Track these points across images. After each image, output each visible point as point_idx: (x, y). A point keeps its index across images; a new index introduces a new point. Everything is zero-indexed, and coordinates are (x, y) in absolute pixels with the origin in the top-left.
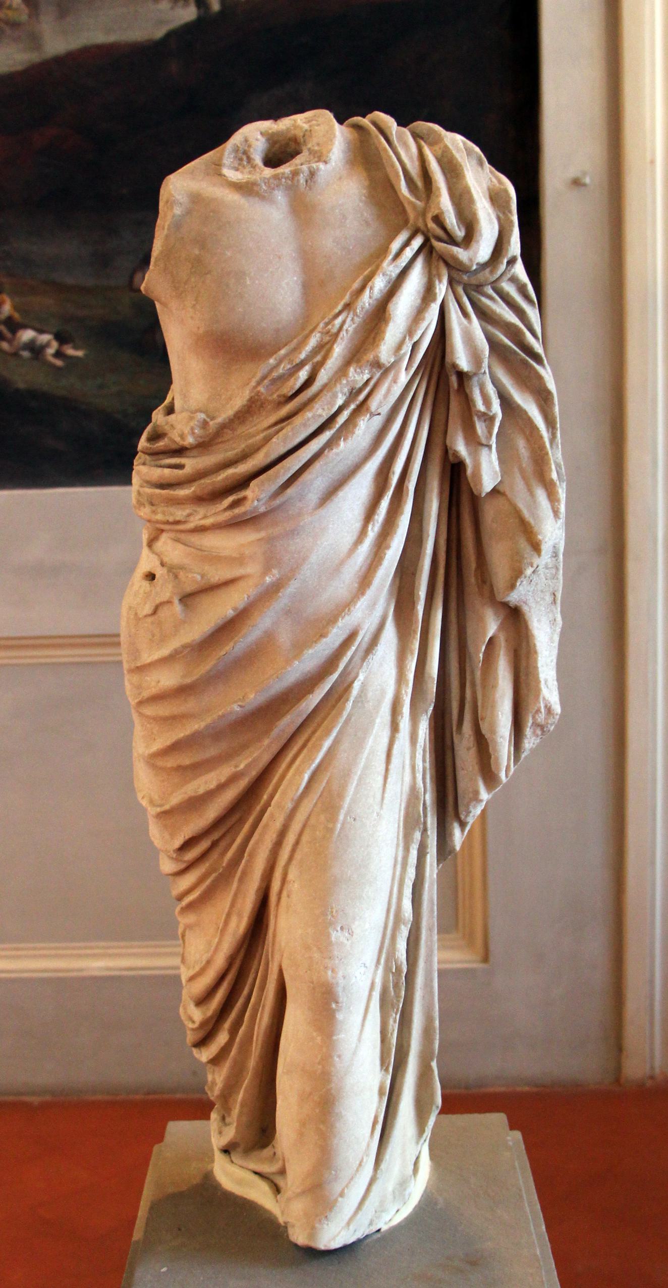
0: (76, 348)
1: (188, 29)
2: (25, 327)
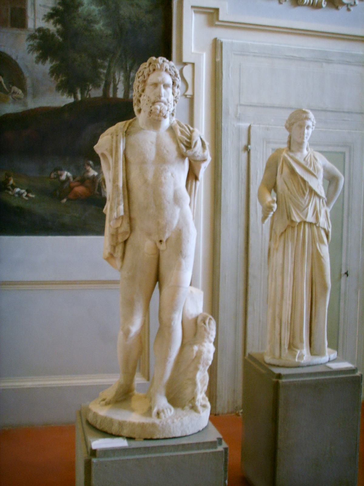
0: (32, 194)
1: (71, 104)
2: (17, 187)
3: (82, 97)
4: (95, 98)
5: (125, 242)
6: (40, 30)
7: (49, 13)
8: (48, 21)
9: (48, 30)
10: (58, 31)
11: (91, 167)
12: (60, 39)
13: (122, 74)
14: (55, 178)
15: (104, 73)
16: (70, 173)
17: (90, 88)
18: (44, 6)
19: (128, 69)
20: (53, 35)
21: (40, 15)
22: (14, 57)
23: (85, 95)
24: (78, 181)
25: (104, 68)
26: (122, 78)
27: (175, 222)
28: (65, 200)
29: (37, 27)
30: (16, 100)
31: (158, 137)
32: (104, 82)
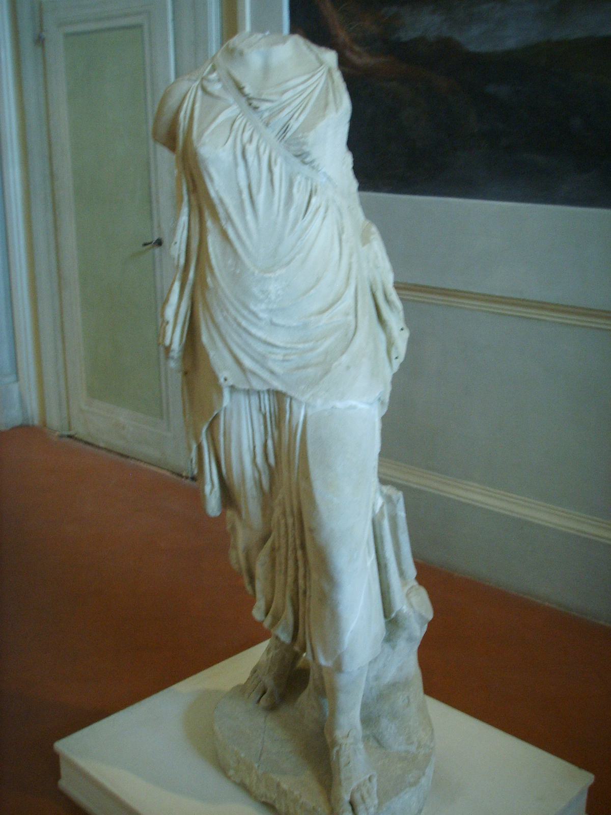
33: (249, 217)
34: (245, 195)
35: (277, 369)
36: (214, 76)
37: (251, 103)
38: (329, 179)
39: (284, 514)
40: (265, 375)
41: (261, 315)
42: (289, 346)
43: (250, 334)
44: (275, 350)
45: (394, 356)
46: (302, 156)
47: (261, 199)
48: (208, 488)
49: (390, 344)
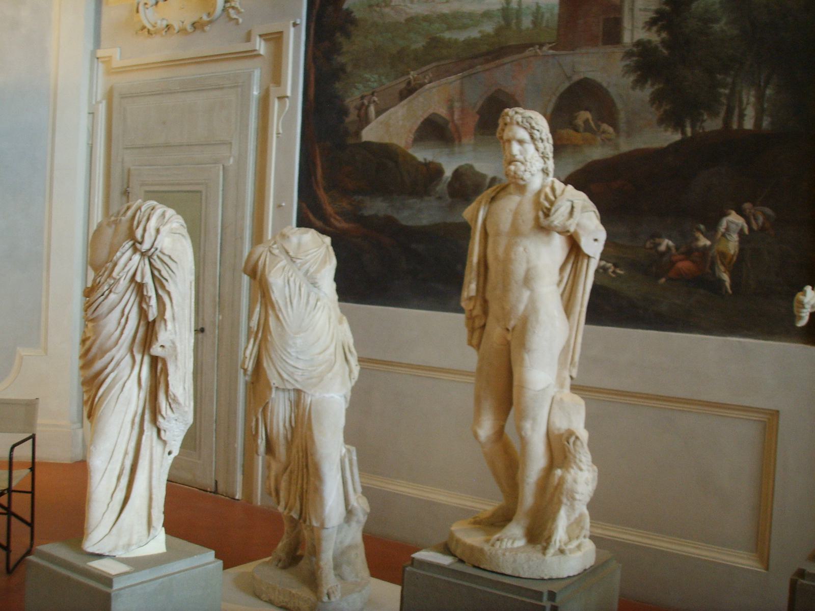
1: (676, 144)
3: (692, 132)
4: (712, 132)
5: (483, 327)
6: (639, 43)
7: (651, 18)
8: (649, 29)
9: (649, 42)
10: (663, 42)
11: (702, 233)
12: (665, 52)
13: (753, 93)
14: (651, 249)
15: (725, 94)
16: (672, 241)
17: (705, 117)
18: (645, 10)
19: (762, 84)
20: (656, 47)
21: (640, 23)
22: (605, 85)
23: (698, 129)
24: (683, 253)
25: (725, 86)
26: (752, 99)
27: (522, 307)
28: (663, 280)
29: (635, 40)
30: (606, 141)
31: (520, 204)
32: (725, 108)
33: (289, 310)
34: (288, 300)
35: (299, 379)
36: (275, 246)
37: (292, 260)
38: (326, 294)
39: (298, 452)
40: (293, 382)
41: (293, 354)
42: (304, 368)
43: (287, 362)
44: (297, 370)
45: (352, 377)
46: (314, 284)
47: (295, 302)
48: (259, 441)
49: (351, 372)
